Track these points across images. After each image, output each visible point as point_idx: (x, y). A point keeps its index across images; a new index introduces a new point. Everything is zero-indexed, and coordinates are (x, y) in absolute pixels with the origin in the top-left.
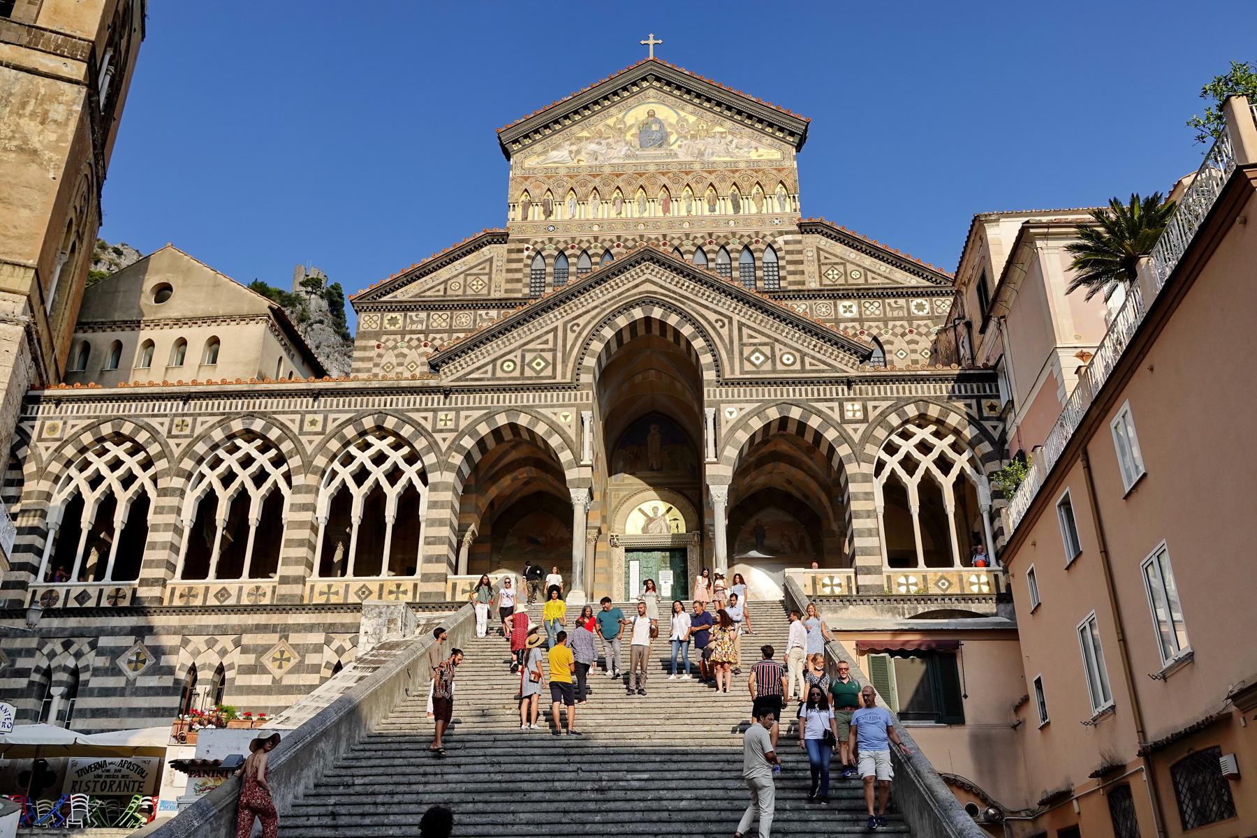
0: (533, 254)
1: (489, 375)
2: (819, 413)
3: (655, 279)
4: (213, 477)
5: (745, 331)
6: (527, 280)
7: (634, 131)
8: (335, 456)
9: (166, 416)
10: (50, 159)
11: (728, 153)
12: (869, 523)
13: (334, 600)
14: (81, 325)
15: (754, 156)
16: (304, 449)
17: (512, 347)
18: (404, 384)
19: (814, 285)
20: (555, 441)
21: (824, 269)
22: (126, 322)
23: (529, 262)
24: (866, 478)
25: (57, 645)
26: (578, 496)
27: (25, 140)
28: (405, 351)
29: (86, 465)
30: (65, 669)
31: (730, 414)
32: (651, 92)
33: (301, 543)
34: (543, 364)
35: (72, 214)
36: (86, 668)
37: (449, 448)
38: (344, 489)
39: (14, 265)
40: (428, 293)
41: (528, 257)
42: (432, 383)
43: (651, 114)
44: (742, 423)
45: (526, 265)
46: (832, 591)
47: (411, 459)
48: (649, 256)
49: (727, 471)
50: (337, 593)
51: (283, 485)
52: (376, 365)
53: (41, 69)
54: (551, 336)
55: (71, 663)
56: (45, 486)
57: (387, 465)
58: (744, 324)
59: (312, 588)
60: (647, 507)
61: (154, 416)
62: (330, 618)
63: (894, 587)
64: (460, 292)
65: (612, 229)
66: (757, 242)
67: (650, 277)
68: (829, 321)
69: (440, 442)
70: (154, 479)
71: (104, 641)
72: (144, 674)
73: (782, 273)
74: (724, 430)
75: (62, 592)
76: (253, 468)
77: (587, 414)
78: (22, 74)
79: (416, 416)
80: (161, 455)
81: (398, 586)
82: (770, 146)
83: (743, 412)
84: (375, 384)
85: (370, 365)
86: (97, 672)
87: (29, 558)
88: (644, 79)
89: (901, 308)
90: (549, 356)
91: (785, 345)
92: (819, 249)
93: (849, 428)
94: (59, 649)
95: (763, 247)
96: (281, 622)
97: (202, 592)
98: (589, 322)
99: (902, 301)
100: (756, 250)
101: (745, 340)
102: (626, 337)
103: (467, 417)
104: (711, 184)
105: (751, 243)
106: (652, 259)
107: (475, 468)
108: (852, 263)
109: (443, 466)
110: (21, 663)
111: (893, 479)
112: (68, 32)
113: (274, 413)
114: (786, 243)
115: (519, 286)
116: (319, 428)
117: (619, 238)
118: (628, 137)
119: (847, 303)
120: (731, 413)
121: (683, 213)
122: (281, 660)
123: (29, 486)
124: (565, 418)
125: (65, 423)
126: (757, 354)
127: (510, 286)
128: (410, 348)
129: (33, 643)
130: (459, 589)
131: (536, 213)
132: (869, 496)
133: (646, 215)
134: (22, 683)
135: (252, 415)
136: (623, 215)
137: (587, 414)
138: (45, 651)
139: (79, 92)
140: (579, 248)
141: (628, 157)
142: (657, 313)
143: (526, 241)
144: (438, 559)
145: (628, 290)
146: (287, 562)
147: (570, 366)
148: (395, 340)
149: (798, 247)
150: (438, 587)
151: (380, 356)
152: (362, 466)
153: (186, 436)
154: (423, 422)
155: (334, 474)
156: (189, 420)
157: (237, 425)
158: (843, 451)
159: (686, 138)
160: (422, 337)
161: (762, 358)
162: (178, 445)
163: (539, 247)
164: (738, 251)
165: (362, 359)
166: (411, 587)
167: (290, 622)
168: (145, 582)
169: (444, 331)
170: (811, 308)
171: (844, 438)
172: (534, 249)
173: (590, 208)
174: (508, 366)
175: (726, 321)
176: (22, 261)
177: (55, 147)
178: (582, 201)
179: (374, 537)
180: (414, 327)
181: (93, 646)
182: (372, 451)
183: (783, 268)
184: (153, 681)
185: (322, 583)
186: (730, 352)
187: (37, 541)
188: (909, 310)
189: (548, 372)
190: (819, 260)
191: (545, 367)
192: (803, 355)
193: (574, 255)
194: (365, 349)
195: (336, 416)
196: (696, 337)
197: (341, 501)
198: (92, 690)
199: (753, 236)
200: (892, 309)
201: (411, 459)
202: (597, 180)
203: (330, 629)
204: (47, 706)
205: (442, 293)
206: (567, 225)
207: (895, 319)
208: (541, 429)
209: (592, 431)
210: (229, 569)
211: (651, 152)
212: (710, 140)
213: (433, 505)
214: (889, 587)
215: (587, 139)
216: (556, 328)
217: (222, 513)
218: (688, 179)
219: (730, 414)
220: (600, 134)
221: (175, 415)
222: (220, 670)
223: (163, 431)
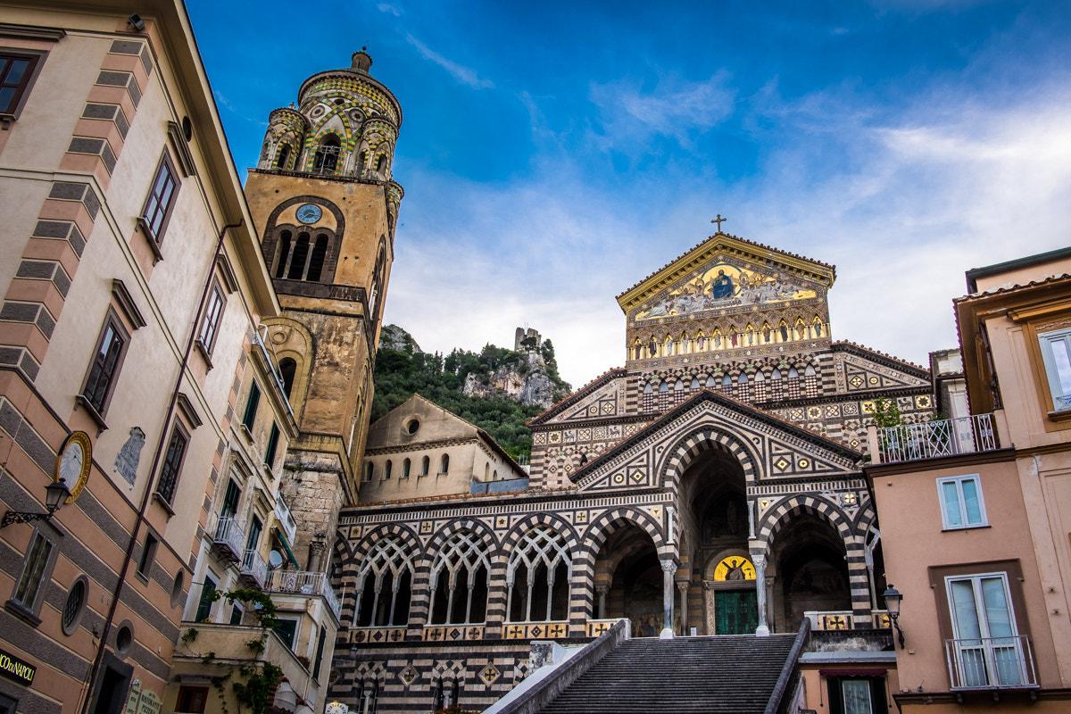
0: (644, 383)
1: (607, 485)
2: (826, 501)
3: (712, 412)
4: (446, 559)
5: (774, 445)
6: (640, 402)
7: (709, 287)
8: (516, 543)
9: (417, 521)
10: (345, 368)
12: (862, 579)
13: (519, 636)
14: (368, 452)
15: (796, 296)
16: (497, 539)
17: (621, 465)
18: (555, 494)
19: (843, 391)
20: (650, 528)
21: (850, 378)
22: (393, 448)
23: (641, 389)
24: (859, 547)
25: (365, 665)
26: (667, 565)
27: (332, 357)
28: (564, 457)
29: (374, 553)
30: (371, 680)
31: (765, 504)
33: (498, 600)
34: (641, 476)
35: (359, 393)
36: (382, 680)
37: (584, 535)
38: (522, 564)
39: (330, 436)
40: (576, 416)
41: (641, 385)
42: (572, 492)
43: (721, 273)
44: (773, 511)
45: (640, 392)
46: (838, 627)
47: (562, 543)
48: (706, 396)
49: (762, 545)
50: (520, 632)
51: (485, 562)
52: (546, 468)
53: (338, 311)
54: (645, 456)
55: (374, 676)
56: (353, 567)
57: (547, 548)
58: (772, 441)
59: (506, 628)
60: (729, 561)
61: (411, 521)
62: (517, 649)
63: (881, 623)
64: (597, 414)
65: (696, 360)
66: (800, 362)
67: (708, 411)
68: (855, 417)
69: (578, 532)
70: (413, 561)
71: (391, 663)
72: (413, 684)
73: (820, 383)
74: (760, 517)
75: (367, 633)
76: (469, 552)
77: (670, 509)
78: (327, 317)
79: (563, 515)
80: (416, 546)
81: (557, 627)
82: (808, 288)
83: (773, 503)
84: (537, 495)
85: (541, 468)
86: (388, 682)
87: (349, 612)
88: (716, 248)
89: (909, 404)
90: (644, 470)
91: (800, 452)
92: (846, 363)
93: (846, 511)
94: (367, 668)
95: (805, 365)
96: (489, 651)
97: (443, 631)
98: (669, 445)
99: (909, 399)
100: (800, 368)
101: (774, 452)
102: (696, 452)
103: (594, 514)
104: (766, 321)
105: (795, 363)
106: (709, 399)
107: (603, 546)
108: (871, 372)
109: (581, 547)
110: (348, 676)
112: (351, 285)
113: (479, 516)
114: (822, 360)
115: (635, 406)
116: (505, 525)
117: (702, 366)
118: (706, 292)
119: (868, 403)
120: (765, 504)
121: (747, 344)
122: (490, 675)
123: (346, 568)
124: (656, 512)
125: (362, 528)
126: (782, 461)
127: (629, 407)
128: (566, 455)
129: (353, 664)
130: (594, 629)
132: (861, 560)
133: (721, 348)
134: (349, 688)
137: (670, 509)
138: (360, 669)
139: (358, 323)
140: (675, 376)
141: (706, 307)
142: (714, 436)
143: (640, 374)
144: (580, 609)
145: (695, 421)
146: (492, 612)
147: (658, 476)
148: (556, 450)
149: (831, 363)
150: (580, 628)
151: (548, 462)
152: (532, 548)
153: (429, 534)
154: (567, 518)
155: (516, 554)
156: (430, 523)
157: (458, 525)
158: (843, 527)
159: (747, 289)
160: (573, 447)
161: (786, 464)
162: (425, 539)
163: (647, 377)
164: (786, 370)
166: (562, 627)
167: (494, 651)
168: (413, 627)
169: (588, 442)
170: (841, 409)
171: (843, 518)
172: (644, 380)
173: (681, 346)
174: (619, 478)
175: (760, 439)
176: (335, 433)
177: (347, 359)
178: (676, 341)
179: (542, 593)
180: (568, 441)
181: (385, 666)
182: (538, 539)
183: (819, 379)
184: (418, 688)
185: (509, 624)
187: (352, 602)
188: (915, 405)
190: (846, 372)
191: (642, 478)
192: (814, 460)
193: (672, 382)
194: (537, 457)
195: (515, 517)
196: (739, 451)
197: (521, 571)
198: (386, 692)
199: (797, 357)
200: (902, 405)
202: (686, 325)
203: (518, 656)
204: (363, 701)
205: (585, 415)
206: (664, 361)
207: (905, 412)
208: (641, 520)
209: (674, 518)
210: (459, 617)
211: (722, 301)
212: (763, 288)
213: (576, 574)
214: (878, 624)
215: (677, 296)
216: (648, 450)
219: (765, 504)
220: (686, 290)
221: (423, 520)
223: (416, 530)
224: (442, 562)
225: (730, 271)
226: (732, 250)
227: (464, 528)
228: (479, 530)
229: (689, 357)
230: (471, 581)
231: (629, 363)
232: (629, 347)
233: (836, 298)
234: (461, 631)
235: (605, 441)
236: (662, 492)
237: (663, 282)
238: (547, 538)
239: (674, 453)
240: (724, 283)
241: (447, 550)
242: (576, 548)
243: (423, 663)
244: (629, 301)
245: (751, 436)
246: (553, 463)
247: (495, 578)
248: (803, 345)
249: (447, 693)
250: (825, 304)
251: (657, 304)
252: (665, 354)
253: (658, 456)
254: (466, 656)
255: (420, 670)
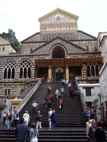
4: (6, 67)
5: (70, 47)
11: (68, 21)
15: (72, 21)
19: (80, 39)
32: (58, 13)
43: (58, 16)
48: (58, 38)
51: (14, 68)
54: (46, 48)
57: (27, 65)
60: (58, 68)
76: (11, 65)
79: (30, 59)
90: (46, 51)
99: (91, 41)
106: (59, 38)
109: (33, 65)
111: (88, 66)
114: (76, 33)
116: (18, 60)
118: (55, 19)
121: (63, 29)
131: (43, 30)
133: (58, 30)
135: (10, 59)
136: (55, 30)
142: (59, 45)
146: (16, 77)
150: (34, 80)
155: (20, 66)
156: (3, 60)
157: (9, 60)
165: (22, 50)
173: (50, 29)
182: (25, 63)
184: (2, 91)
185: (20, 79)
186: (68, 50)
189: (46, 53)
192: (77, 50)
194: (22, 48)
197: (21, 69)
201: (30, 64)
206: (47, 31)
210: (9, 78)
211: (58, 21)
213: (32, 70)
217: (8, 71)
218: (63, 25)
222: (9, 90)
224: (5, 67)
225: (60, 16)
226: (60, 12)
227: (10, 61)
228: (13, 61)
229: (52, 31)
230: (11, 71)
231: (40, 32)
232: (40, 29)
233: (78, 22)
234: (10, 80)
235: (36, 46)
236: (49, 55)
237: (47, 17)
238: (27, 63)
239: (52, 48)
240: (59, 18)
241: (6, 65)
242: (32, 65)
243: (2, 86)
244: (40, 20)
245: (66, 45)
246: (25, 50)
247: (16, 70)
248: (73, 30)
249: (7, 92)
250: (77, 24)
251: (46, 21)
252: (47, 30)
253: (49, 48)
254: (12, 85)
255: (2, 87)
